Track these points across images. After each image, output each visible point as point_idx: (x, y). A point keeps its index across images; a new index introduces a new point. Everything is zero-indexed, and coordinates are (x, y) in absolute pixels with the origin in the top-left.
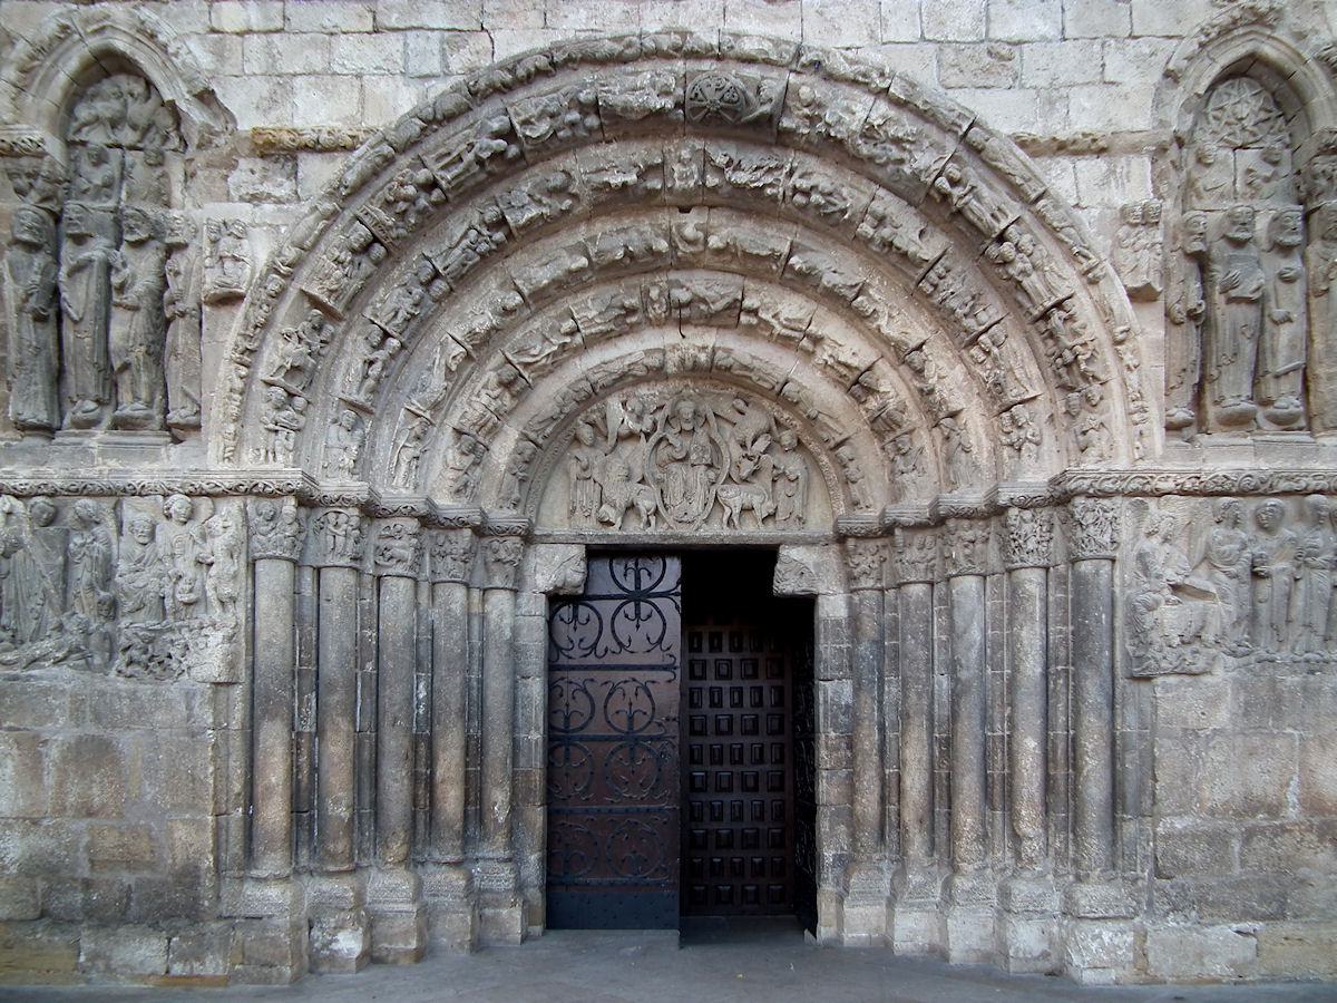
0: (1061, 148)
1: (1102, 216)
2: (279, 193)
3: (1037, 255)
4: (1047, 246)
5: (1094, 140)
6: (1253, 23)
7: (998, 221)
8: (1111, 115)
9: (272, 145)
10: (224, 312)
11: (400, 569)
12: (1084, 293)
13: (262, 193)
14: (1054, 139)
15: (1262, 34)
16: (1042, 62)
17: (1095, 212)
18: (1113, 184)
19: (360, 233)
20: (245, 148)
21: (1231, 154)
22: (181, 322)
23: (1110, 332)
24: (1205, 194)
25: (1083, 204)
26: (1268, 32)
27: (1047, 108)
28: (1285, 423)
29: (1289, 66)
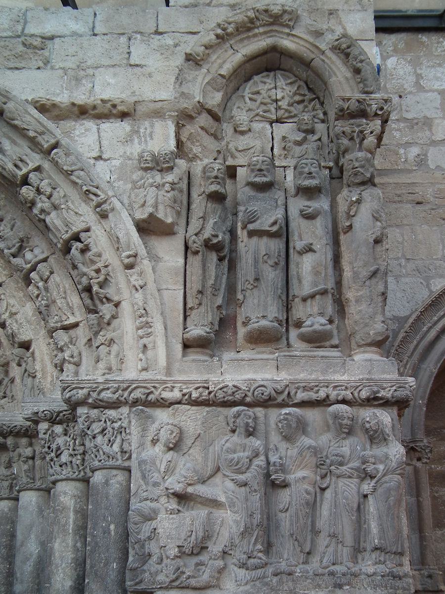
0: (83, 112)
1: (122, 166)
3: (55, 195)
4: (64, 188)
5: (114, 106)
6: (272, 24)
7: (21, 169)
8: (134, 89)
12: (99, 227)
14: (73, 104)
15: (282, 32)
16: (71, 50)
17: (116, 163)
18: (136, 141)
21: (268, 126)
23: (120, 256)
24: (237, 154)
25: (104, 156)
26: (287, 30)
27: (74, 82)
28: (316, 340)
29: (307, 54)
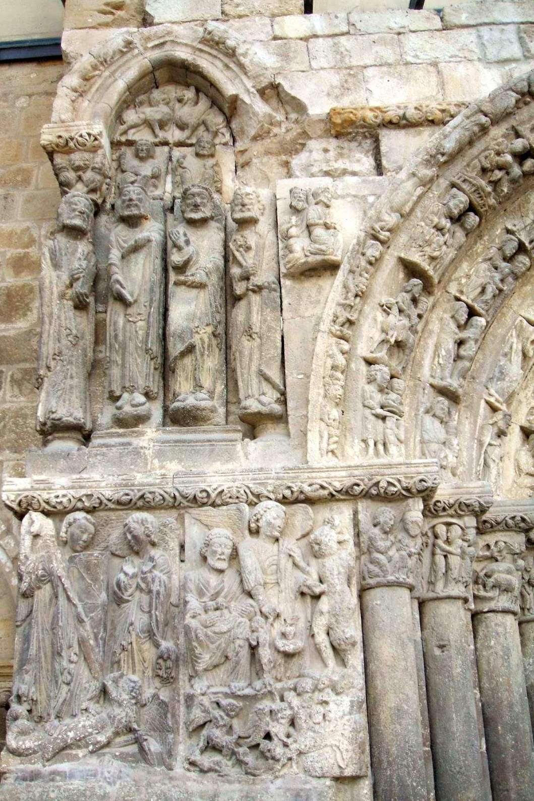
2: (356, 167)
9: (352, 123)
10: (310, 286)
11: (504, 601)
13: (336, 169)
19: (460, 201)
20: (319, 129)
22: (255, 299)
